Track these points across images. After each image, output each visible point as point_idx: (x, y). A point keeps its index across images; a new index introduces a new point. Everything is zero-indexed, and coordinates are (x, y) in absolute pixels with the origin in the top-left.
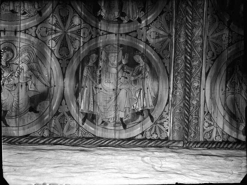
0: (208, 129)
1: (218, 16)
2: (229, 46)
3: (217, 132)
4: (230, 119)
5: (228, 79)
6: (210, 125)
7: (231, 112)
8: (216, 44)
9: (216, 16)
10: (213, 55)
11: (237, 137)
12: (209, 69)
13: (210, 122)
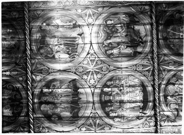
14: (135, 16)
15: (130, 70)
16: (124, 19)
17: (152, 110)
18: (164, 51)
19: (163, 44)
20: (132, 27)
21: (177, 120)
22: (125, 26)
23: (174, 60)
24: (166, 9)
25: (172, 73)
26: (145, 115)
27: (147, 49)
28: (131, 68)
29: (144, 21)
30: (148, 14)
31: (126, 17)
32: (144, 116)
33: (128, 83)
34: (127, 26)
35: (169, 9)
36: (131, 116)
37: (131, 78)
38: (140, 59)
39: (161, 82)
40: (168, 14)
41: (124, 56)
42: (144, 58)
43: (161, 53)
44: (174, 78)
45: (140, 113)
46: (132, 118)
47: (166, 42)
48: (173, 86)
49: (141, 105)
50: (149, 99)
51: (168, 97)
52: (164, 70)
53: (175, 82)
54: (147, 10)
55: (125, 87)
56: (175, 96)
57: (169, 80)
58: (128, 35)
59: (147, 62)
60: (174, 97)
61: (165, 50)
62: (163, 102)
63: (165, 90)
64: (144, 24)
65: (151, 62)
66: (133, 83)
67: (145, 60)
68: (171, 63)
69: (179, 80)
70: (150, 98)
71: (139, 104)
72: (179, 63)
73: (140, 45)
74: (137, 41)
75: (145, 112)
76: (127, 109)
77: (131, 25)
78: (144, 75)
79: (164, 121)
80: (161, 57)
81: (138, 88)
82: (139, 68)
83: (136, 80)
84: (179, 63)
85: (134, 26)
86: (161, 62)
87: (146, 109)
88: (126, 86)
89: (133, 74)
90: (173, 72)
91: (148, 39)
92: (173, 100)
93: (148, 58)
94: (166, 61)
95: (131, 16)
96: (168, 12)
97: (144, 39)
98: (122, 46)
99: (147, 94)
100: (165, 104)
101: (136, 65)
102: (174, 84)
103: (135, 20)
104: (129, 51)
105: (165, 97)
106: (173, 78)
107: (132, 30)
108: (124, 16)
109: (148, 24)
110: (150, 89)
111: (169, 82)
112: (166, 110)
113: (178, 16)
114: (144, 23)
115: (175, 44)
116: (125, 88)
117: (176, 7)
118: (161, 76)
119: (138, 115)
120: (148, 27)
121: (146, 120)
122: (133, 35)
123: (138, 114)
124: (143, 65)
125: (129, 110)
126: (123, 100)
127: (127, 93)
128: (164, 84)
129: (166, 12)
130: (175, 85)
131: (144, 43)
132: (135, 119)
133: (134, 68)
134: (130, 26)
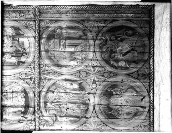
0: (143, 127)
1: (83, 124)
2: (98, 118)
3: (144, 123)
4: (138, 116)
5: (115, 117)
6: (141, 126)
7: (133, 116)
8: (98, 124)
9: (83, 125)
10: (104, 126)
11: (146, 112)
12: (111, 128)
13: (139, 126)
14: (20, 30)
15: (14, 77)
16: (10, 31)
17: (33, 114)
18: (45, 61)
19: (45, 55)
20: (17, 39)
21: (54, 124)
22: (10, 38)
23: (54, 71)
24: (49, 25)
25: (52, 82)
26: (26, 119)
27: (30, 59)
28: (14, 75)
29: (28, 34)
30: (32, 29)
31: (12, 30)
32: (25, 120)
33: (12, 89)
34: (12, 38)
35: (51, 25)
36: (13, 119)
37: (14, 85)
38: (23, 68)
39: (41, 90)
40: (50, 29)
41: (8, 64)
42: (27, 68)
43: (42, 64)
44: (54, 87)
45: (22, 117)
46: (14, 121)
47: (47, 54)
48: (52, 93)
49: (23, 109)
50: (30, 105)
51: (47, 104)
52: (45, 79)
53: (54, 90)
54: (32, 25)
55: (9, 93)
56: (54, 103)
57: (49, 88)
58: (13, 46)
59: (29, 71)
60: (53, 104)
61: (46, 61)
62: (43, 108)
63: (45, 97)
64: (28, 37)
65: (34, 71)
66: (15, 90)
67: (28, 69)
68: (51, 72)
69: (58, 89)
70: (31, 104)
71: (20, 109)
72: (58, 73)
73: (24, 55)
74: (20, 52)
75: (26, 116)
76: (9, 113)
77: (16, 37)
78: (27, 83)
79: (44, 125)
80: (43, 67)
81: (20, 94)
82: (22, 76)
83: (19, 87)
84: (58, 73)
85: (19, 38)
86: (42, 72)
87: (28, 113)
88: (10, 92)
89: (16, 81)
90: (53, 81)
91: (31, 51)
92: (52, 107)
93: (31, 67)
94: (47, 71)
95: (17, 29)
96: (50, 28)
97: (28, 51)
98: (8, 56)
99: (29, 100)
100: (45, 110)
101: (19, 73)
102: (53, 92)
103: (19, 33)
104: (14, 60)
105: (45, 103)
106: (53, 86)
107: (16, 42)
108: (10, 29)
109: (31, 37)
110: (31, 95)
111: (49, 90)
112: (45, 115)
113: (60, 31)
114: (28, 36)
115: (55, 55)
116: (8, 94)
117: (57, 23)
118: (42, 84)
119: (20, 119)
120: (32, 40)
121: (27, 123)
122: (18, 46)
123: (19, 118)
124: (25, 74)
125: (11, 114)
126: (6, 105)
127: (11, 98)
128: (44, 92)
129: (48, 27)
130: (54, 93)
131: (28, 54)
132: (16, 122)
133: (17, 76)
134: (15, 38)
